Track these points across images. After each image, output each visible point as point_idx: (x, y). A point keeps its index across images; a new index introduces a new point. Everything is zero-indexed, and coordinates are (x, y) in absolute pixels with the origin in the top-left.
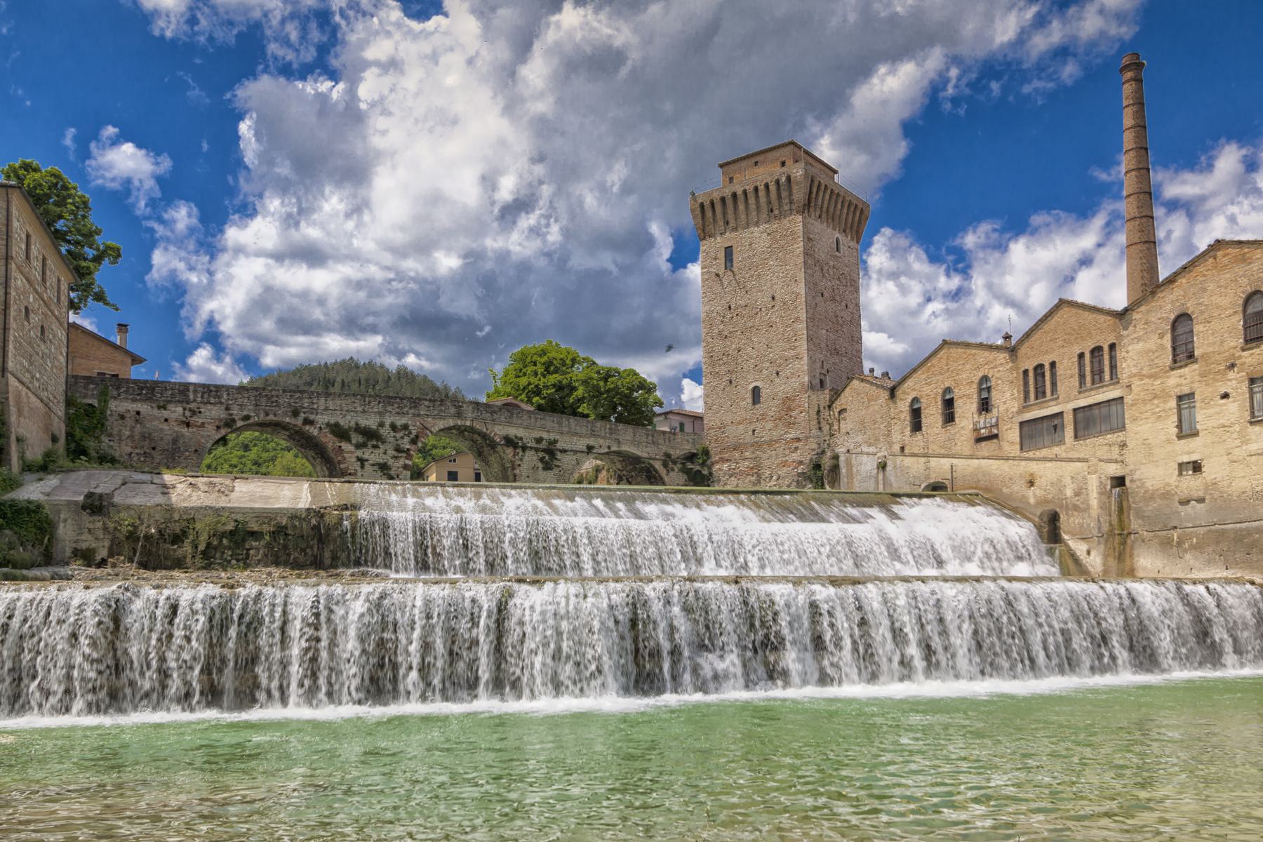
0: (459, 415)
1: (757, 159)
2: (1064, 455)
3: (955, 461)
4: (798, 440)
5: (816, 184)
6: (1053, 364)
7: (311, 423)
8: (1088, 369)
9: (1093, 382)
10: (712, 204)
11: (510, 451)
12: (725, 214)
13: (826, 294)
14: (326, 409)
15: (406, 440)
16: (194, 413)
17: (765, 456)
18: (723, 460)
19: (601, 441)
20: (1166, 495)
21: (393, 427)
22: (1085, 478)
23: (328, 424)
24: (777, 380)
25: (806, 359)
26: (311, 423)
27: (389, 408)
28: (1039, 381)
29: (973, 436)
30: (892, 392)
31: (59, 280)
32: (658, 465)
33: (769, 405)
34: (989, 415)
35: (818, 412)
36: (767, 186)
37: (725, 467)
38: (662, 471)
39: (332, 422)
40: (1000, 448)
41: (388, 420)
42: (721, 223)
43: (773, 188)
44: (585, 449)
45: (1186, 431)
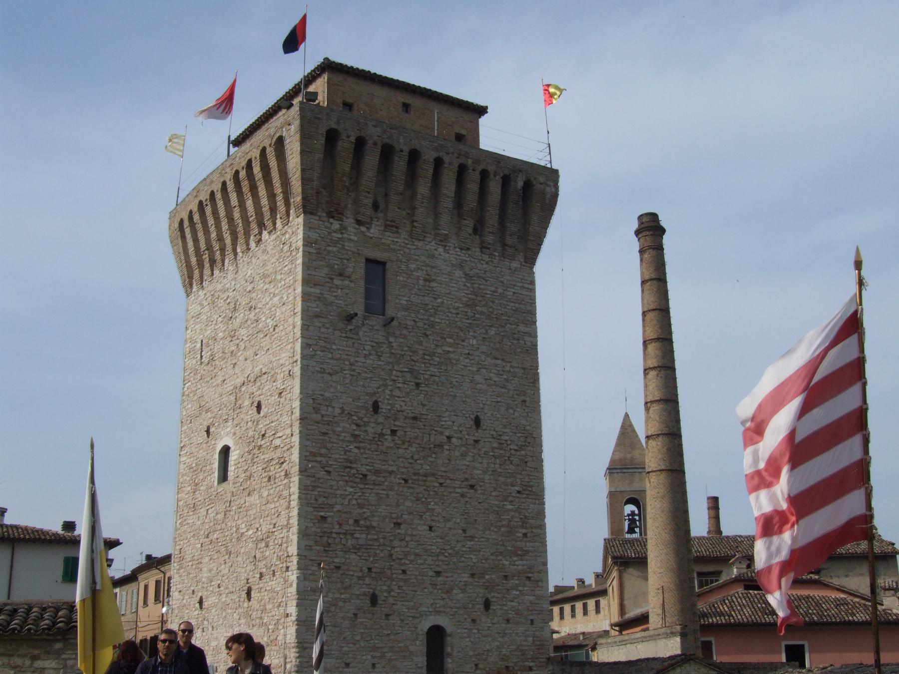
10: (360, 144)
24: (485, 621)
42: (368, 201)
43: (495, 187)
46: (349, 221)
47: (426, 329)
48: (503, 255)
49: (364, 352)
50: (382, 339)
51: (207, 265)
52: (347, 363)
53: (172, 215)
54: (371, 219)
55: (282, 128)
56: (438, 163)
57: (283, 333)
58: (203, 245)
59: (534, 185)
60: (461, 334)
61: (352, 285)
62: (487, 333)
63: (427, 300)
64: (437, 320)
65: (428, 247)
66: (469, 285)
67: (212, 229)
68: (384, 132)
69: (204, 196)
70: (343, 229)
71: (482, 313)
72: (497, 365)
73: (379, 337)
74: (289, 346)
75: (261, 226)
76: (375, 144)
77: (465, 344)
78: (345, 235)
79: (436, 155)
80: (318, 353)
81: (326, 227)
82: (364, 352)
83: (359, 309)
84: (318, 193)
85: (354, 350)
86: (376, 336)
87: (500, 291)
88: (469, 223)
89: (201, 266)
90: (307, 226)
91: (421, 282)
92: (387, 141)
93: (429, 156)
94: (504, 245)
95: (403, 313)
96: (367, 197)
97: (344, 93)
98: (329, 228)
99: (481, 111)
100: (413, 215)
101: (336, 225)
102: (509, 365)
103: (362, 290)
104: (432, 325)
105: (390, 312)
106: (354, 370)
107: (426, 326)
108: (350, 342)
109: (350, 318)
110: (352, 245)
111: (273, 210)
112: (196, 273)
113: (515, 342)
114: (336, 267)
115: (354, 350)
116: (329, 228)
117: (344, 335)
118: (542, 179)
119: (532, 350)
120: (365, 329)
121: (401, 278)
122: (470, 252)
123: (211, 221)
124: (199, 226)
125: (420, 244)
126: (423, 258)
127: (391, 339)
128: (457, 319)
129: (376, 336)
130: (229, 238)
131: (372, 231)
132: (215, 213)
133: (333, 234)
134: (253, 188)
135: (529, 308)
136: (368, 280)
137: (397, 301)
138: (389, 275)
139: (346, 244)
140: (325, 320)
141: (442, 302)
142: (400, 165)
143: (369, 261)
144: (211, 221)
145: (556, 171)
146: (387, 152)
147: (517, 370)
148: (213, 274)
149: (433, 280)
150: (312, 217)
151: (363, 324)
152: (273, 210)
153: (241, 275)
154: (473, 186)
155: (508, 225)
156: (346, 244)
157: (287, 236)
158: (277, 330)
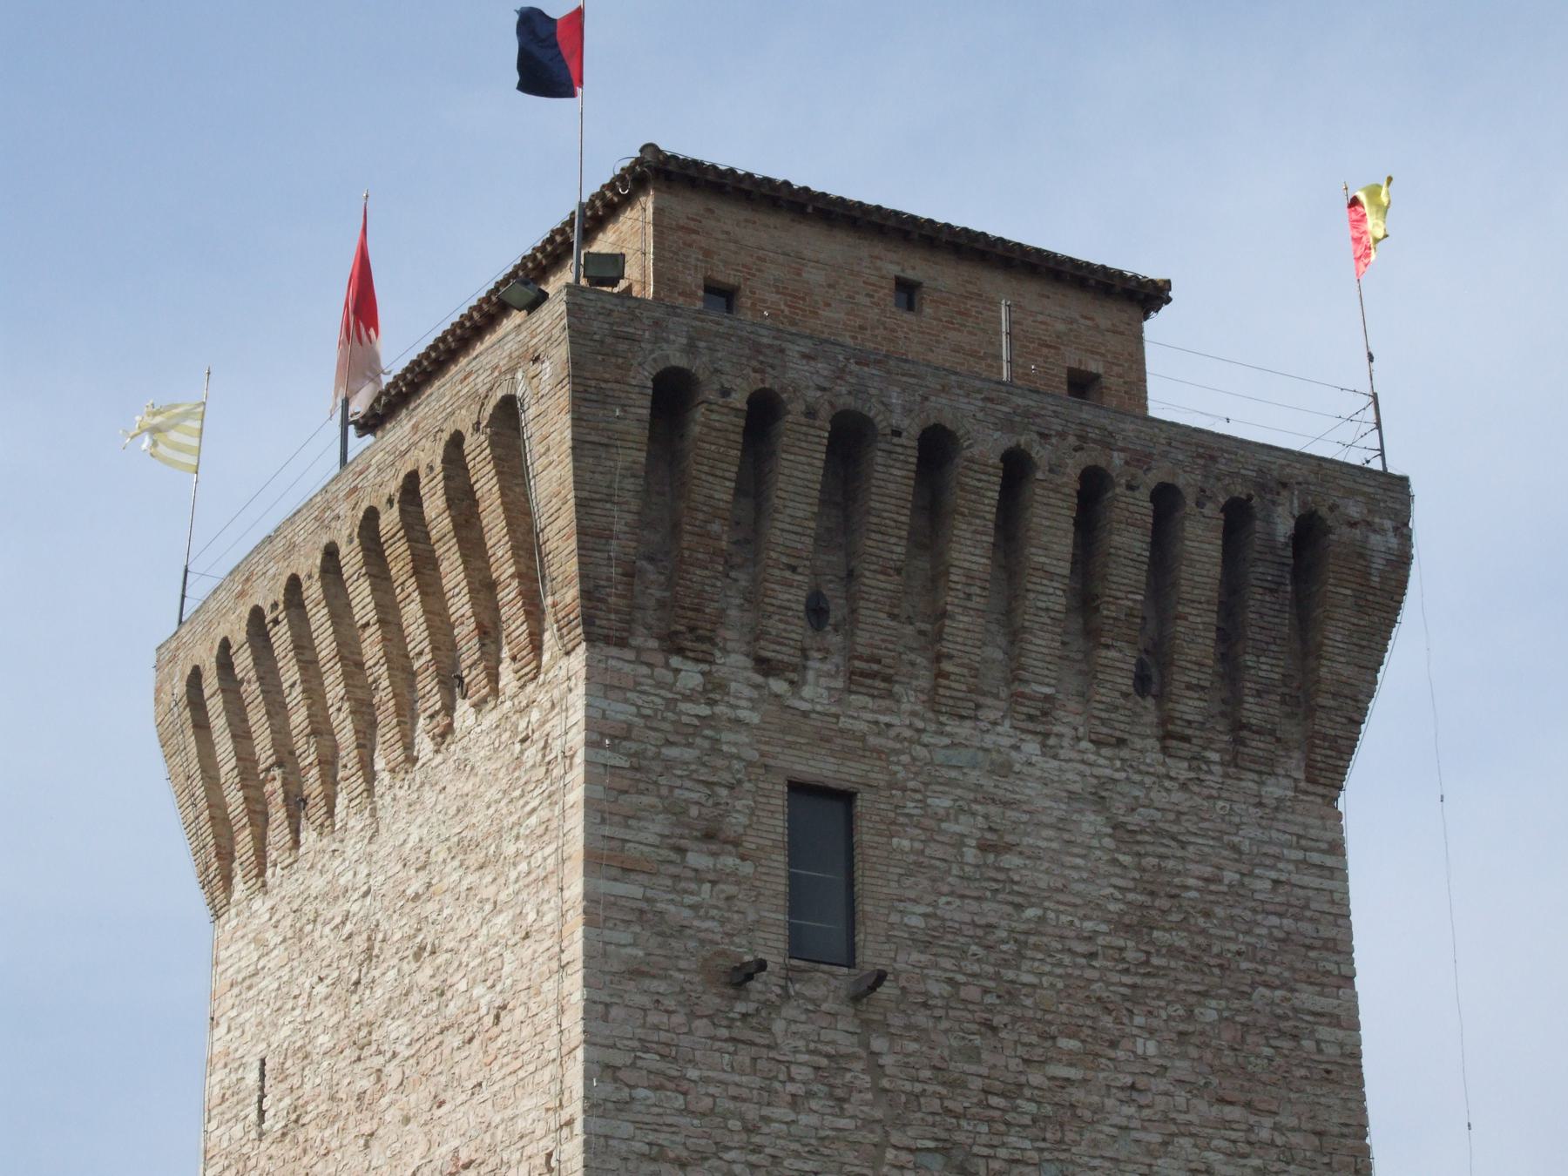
1: (917, 267)
10: (763, 413)
42: (794, 598)
43: (1201, 541)
46: (734, 664)
47: (990, 1009)
48: (1234, 761)
49: (791, 1088)
50: (846, 1044)
51: (278, 814)
52: (735, 1124)
53: (166, 655)
54: (804, 653)
55: (512, 370)
56: (1016, 467)
57: (527, 1031)
58: (264, 750)
59: (1329, 531)
60: (1107, 1021)
61: (747, 868)
62: (1190, 1015)
63: (991, 911)
64: (1027, 978)
65: (989, 740)
66: (1126, 859)
67: (295, 698)
68: (840, 374)
69: (267, 594)
70: (714, 689)
71: (1173, 952)
72: (1226, 1124)
73: (840, 1038)
74: (546, 1074)
75: (452, 683)
76: (811, 413)
77: (1120, 1054)
78: (720, 709)
79: (1006, 441)
80: (641, 1093)
81: (659, 685)
82: (791, 1088)
83: (772, 946)
84: (630, 574)
85: (757, 1081)
86: (827, 1035)
87: (1230, 876)
88: (1119, 660)
89: (258, 815)
90: (600, 684)
91: (971, 855)
92: (846, 402)
93: (984, 445)
94: (1238, 727)
95: (915, 956)
96: (788, 584)
97: (708, 253)
98: (670, 687)
99: (1149, 296)
100: (939, 637)
101: (691, 676)
102: (1268, 1122)
103: (781, 885)
104: (1011, 995)
105: (871, 954)
106: (758, 1150)
107: (989, 999)
108: (744, 1057)
109: (743, 976)
110: (743, 738)
111: (489, 632)
112: (244, 843)
113: (1286, 1044)
114: (694, 811)
115: (757, 1081)
116: (671, 687)
117: (724, 1033)
118: (1354, 510)
119: (1344, 1072)
120: (789, 1011)
121: (906, 843)
122: (1125, 753)
123: (290, 673)
124: (252, 690)
125: (964, 730)
126: (974, 776)
127: (878, 1044)
128: (1089, 974)
129: (827, 1035)
130: (349, 725)
131: (807, 691)
132: (303, 645)
133: (683, 706)
134: (425, 566)
135: (1328, 932)
136: (796, 851)
137: (894, 918)
138: (865, 834)
139: (726, 736)
140: (662, 987)
141: (1042, 919)
142: (891, 477)
143: (799, 789)
144: (290, 673)
145: (1403, 482)
146: (850, 439)
147: (1296, 1139)
148: (296, 843)
149: (1009, 848)
150: (614, 651)
151: (786, 996)
152: (489, 632)
153: (387, 841)
154: (1128, 540)
155: (1249, 659)
156: (726, 736)
157: (535, 715)
158: (506, 1021)
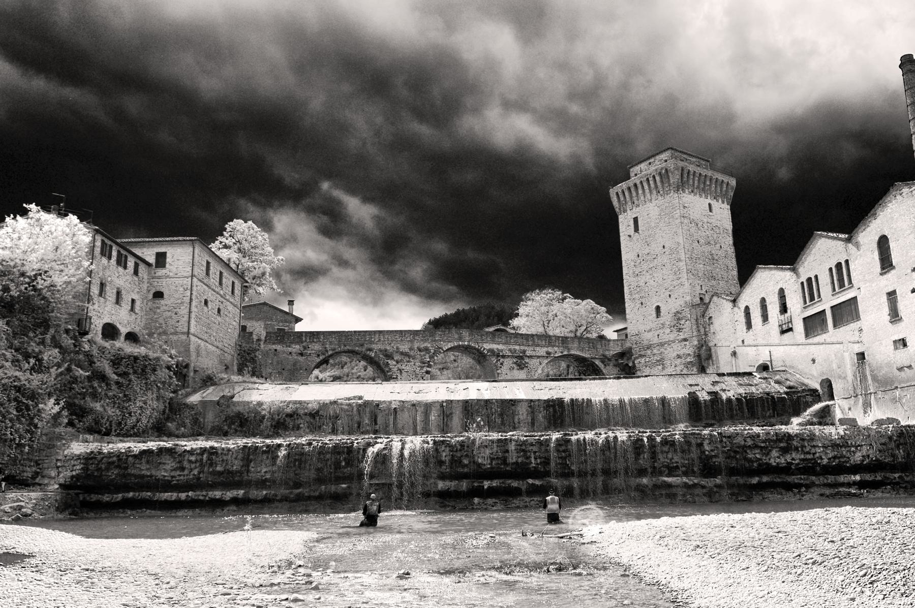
0: (460, 339)
2: (828, 340)
3: (772, 348)
4: (685, 340)
5: (686, 172)
6: (816, 277)
7: (370, 350)
8: (835, 278)
9: (840, 288)
11: (494, 360)
12: (631, 197)
13: (702, 241)
14: (379, 340)
15: (427, 356)
16: (305, 348)
17: (666, 352)
18: (641, 356)
19: (556, 349)
20: (889, 365)
21: (420, 350)
22: (842, 355)
23: (381, 351)
24: (669, 300)
25: (687, 284)
26: (370, 350)
27: (417, 338)
28: (810, 289)
29: (777, 330)
30: (734, 301)
31: (233, 283)
32: (597, 362)
33: (666, 317)
34: (786, 315)
35: (697, 320)
36: (654, 177)
37: (643, 360)
38: (601, 365)
39: (383, 348)
40: (794, 338)
41: (416, 345)
43: (658, 178)
44: (545, 354)
45: (895, 316)
88: (654, 192)
93: (638, 182)
154: (651, 182)
